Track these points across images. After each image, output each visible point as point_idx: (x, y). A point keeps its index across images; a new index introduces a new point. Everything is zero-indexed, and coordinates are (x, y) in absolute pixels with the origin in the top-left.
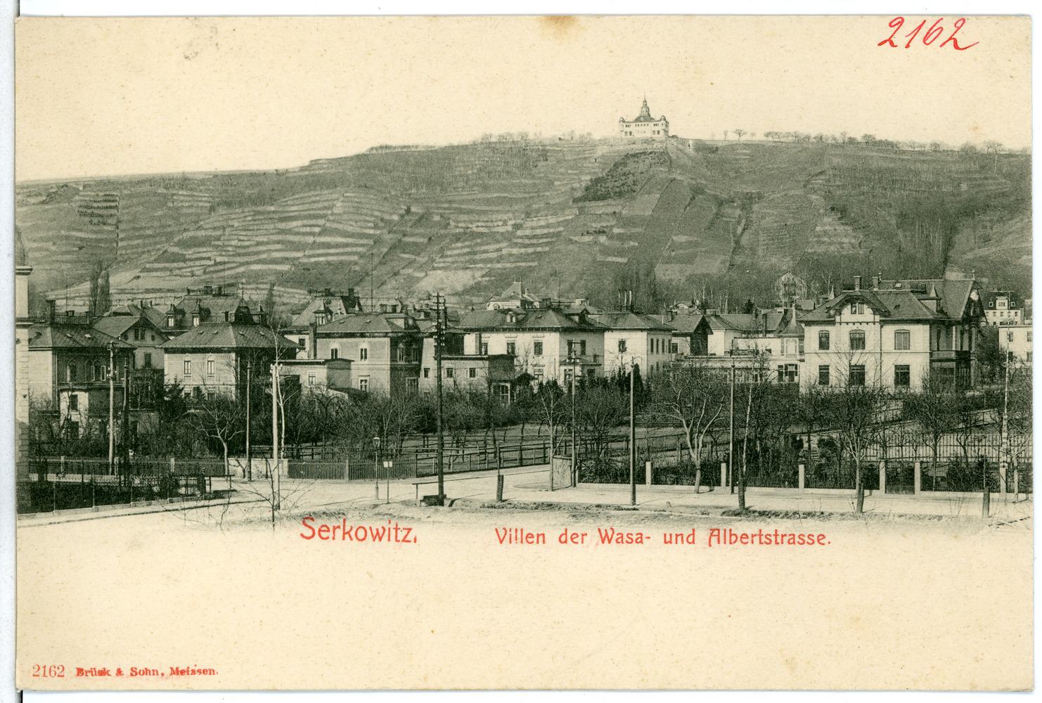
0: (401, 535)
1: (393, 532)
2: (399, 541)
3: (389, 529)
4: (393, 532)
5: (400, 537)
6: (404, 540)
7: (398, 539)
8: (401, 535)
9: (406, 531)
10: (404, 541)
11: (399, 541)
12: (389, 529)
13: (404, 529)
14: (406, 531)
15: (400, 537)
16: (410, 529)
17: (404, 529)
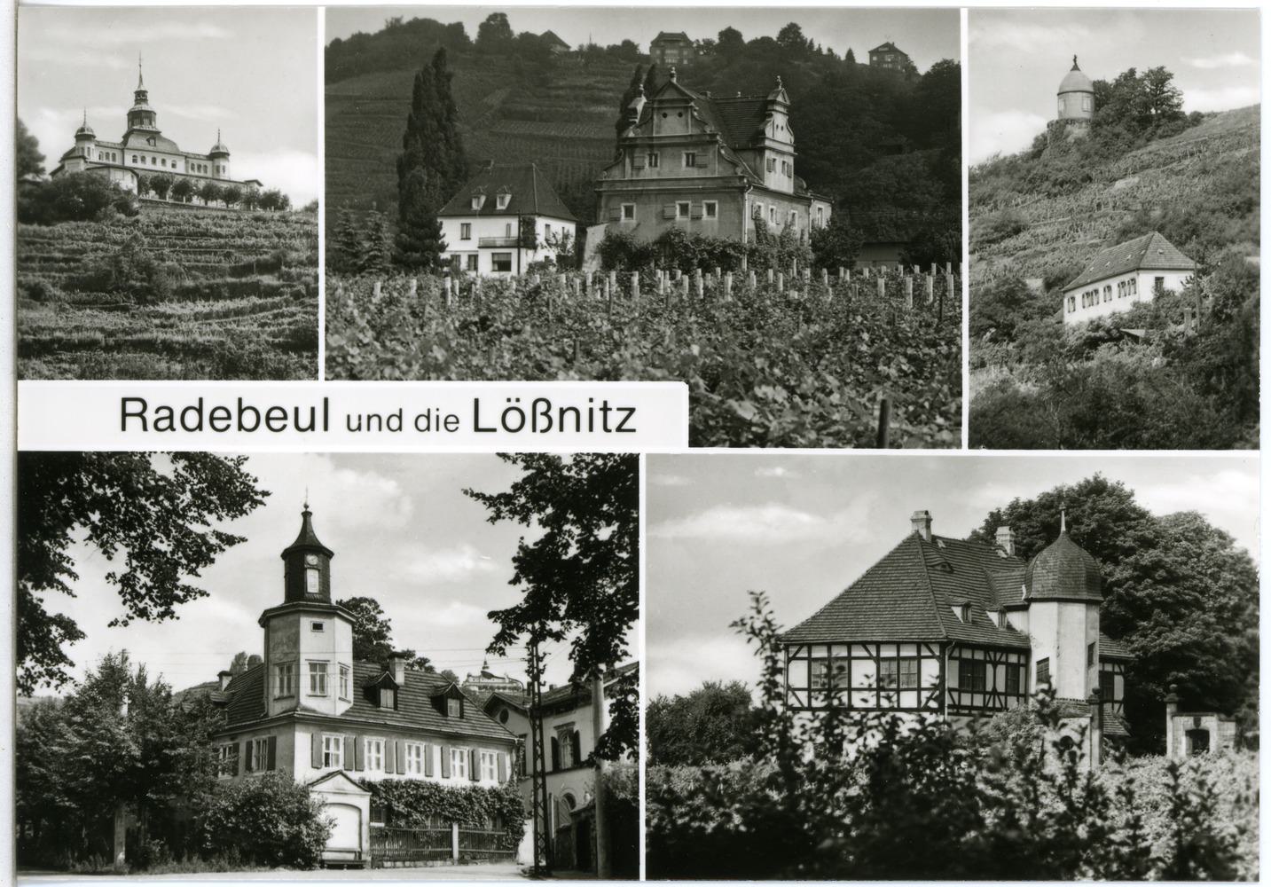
0: (615, 418)
1: (598, 416)
2: (610, 431)
3: (591, 410)
4: (598, 416)
5: (612, 424)
6: (619, 429)
7: (609, 428)
8: (615, 418)
9: (625, 413)
10: (619, 429)
11: (610, 431)
12: (591, 410)
13: (619, 409)
14: (625, 413)
15: (612, 424)
16: (632, 411)
17: (619, 409)
